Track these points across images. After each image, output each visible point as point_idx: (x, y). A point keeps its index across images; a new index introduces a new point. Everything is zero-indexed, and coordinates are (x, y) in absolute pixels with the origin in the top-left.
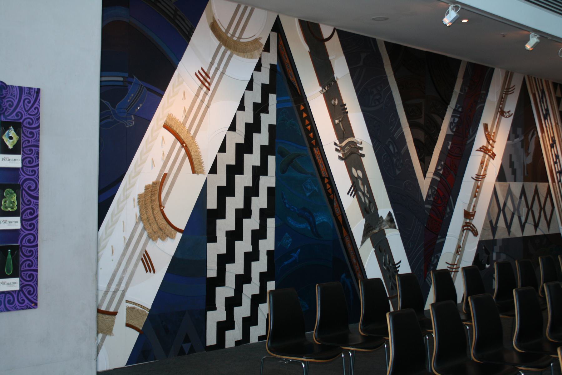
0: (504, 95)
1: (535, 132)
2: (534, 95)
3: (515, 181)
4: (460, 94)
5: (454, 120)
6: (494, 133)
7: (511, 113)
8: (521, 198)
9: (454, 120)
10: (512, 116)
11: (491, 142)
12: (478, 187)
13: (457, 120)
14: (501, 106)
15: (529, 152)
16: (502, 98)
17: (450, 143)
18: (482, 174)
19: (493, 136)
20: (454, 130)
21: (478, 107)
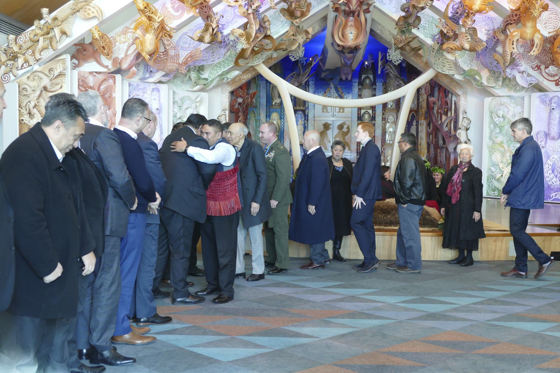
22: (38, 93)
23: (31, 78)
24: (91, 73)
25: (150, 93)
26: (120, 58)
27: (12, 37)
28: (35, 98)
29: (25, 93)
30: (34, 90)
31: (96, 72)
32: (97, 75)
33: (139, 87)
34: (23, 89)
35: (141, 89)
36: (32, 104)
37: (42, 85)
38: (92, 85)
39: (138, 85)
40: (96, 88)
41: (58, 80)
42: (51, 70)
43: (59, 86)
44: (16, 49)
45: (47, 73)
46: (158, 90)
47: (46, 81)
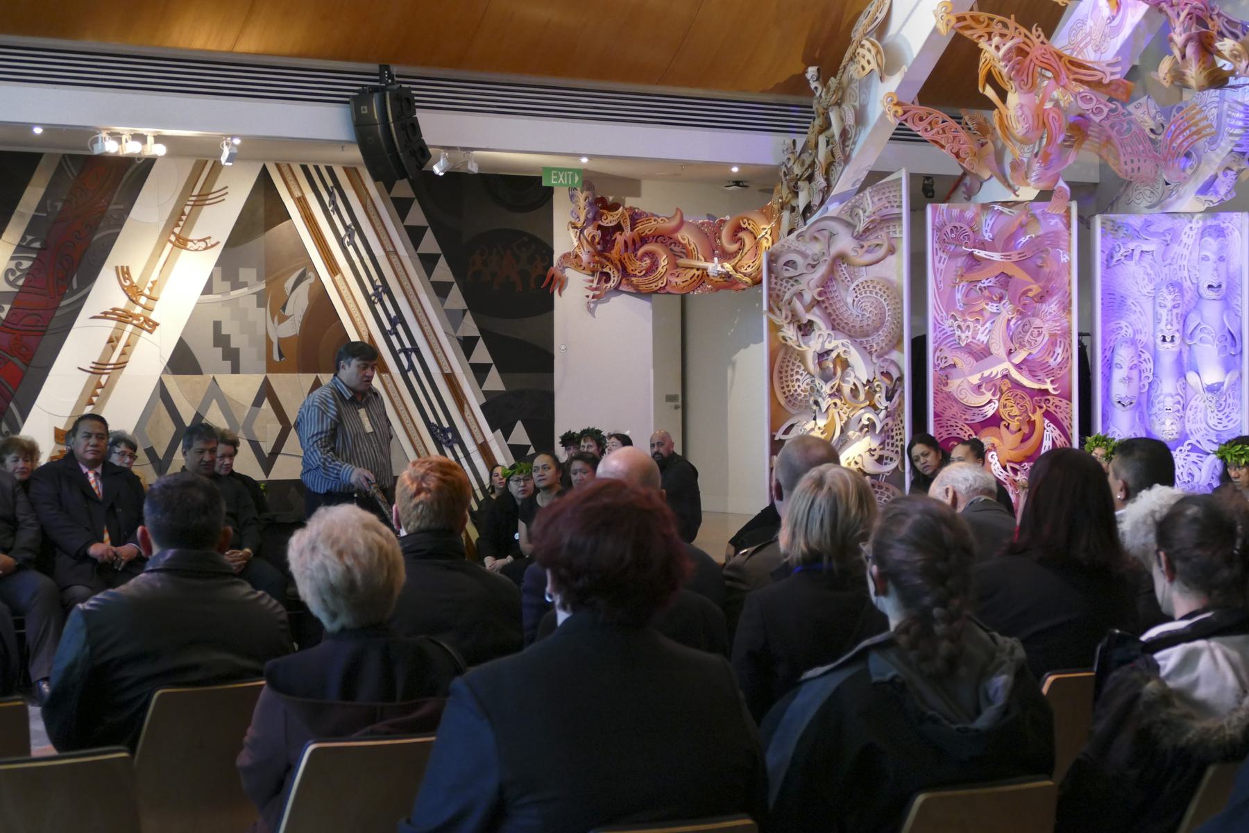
0: (187, 210)
1: (311, 274)
2: (302, 203)
3: (235, 370)
4: (34, 218)
5: (19, 264)
6: (154, 283)
7: (210, 242)
8: (257, 403)
9: (20, 264)
10: (220, 247)
11: (143, 300)
12: (99, 386)
13: (26, 264)
14: (177, 230)
15: (288, 311)
16: (183, 213)
17: (7, 307)
18: (114, 360)
19: (151, 289)
20: (20, 282)
21: (96, 237)
22: (822, 270)
23: (807, 236)
24: (986, 207)
25: (1190, 241)
26: (1025, 160)
27: (787, 139)
28: (812, 284)
29: (791, 272)
30: (814, 266)
31: (1005, 204)
32: (1006, 210)
33: (1152, 229)
34: (790, 264)
35: (1154, 234)
36: (808, 297)
37: (834, 250)
38: (987, 236)
39: (1148, 224)
40: (1000, 244)
41: (881, 237)
42: (852, 211)
43: (881, 252)
44: (797, 170)
45: (850, 220)
46: (1220, 233)
47: (844, 242)
